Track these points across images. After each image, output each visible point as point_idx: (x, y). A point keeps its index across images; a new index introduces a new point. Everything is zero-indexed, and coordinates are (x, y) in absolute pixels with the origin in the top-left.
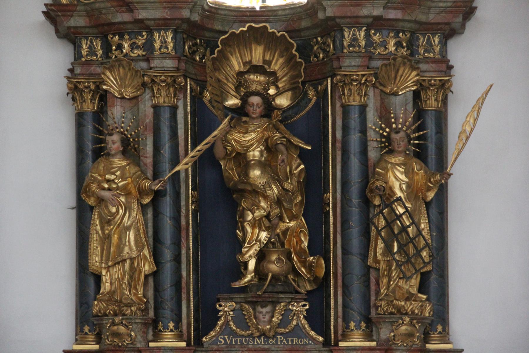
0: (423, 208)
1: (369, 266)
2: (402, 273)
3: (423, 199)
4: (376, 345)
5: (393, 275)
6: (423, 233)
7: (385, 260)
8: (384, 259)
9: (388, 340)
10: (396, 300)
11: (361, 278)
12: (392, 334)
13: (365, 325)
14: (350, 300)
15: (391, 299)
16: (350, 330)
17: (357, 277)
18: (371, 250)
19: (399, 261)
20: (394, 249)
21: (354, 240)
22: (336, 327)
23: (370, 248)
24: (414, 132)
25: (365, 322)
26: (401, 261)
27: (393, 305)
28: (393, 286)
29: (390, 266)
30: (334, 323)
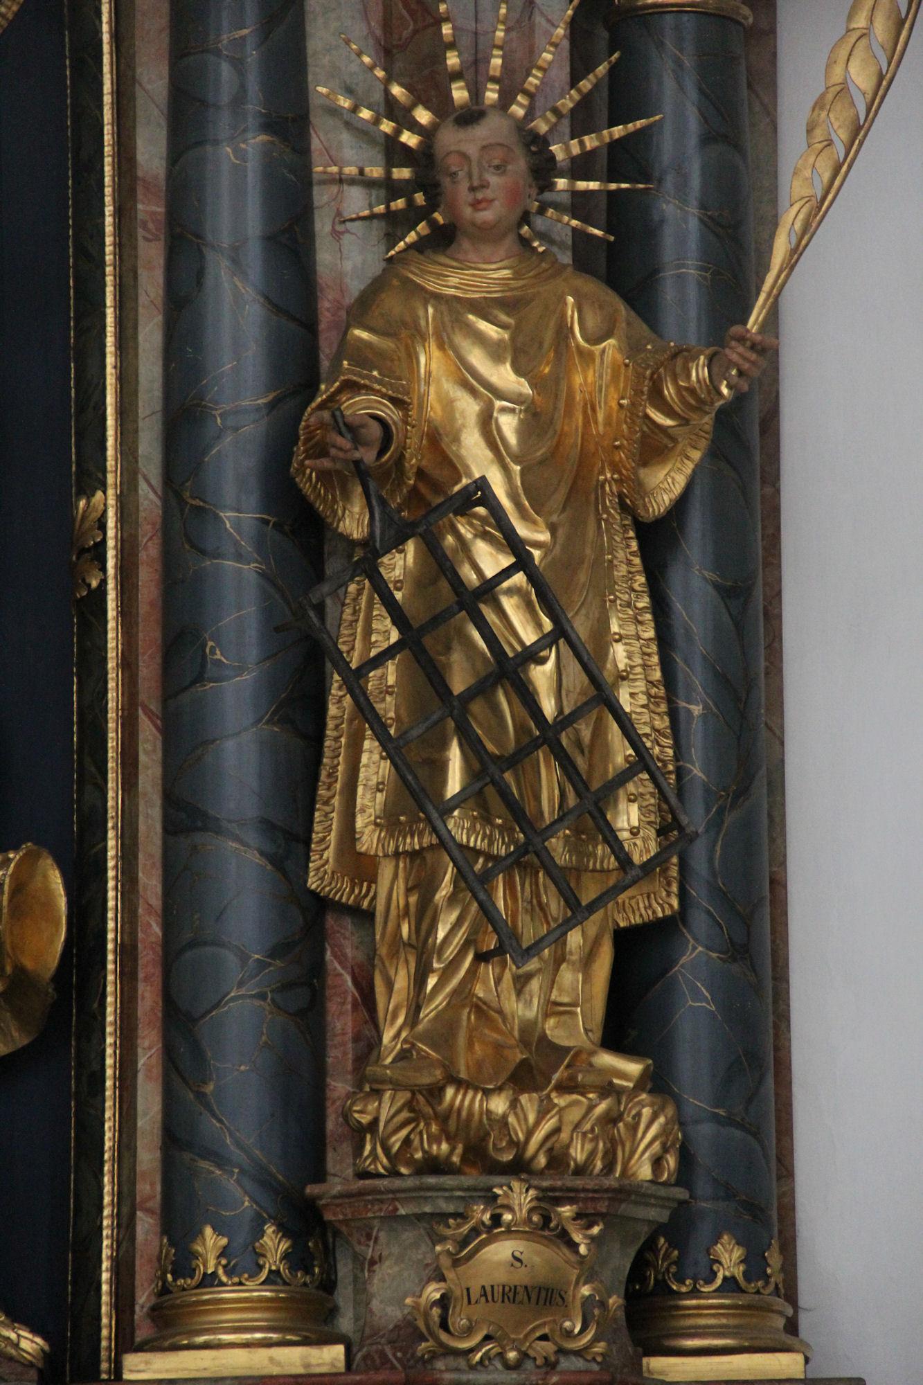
0: (621, 555)
1: (314, 894)
2: (495, 930)
3: (624, 508)
4: (341, 1366)
5: (441, 935)
6: (624, 698)
7: (397, 854)
8: (391, 849)
9: (409, 1332)
10: (460, 1084)
11: (262, 965)
12: (433, 1292)
13: (284, 1245)
14: (200, 1096)
15: (425, 1080)
16: (198, 1276)
17: (244, 958)
18: (327, 802)
19: (477, 853)
20: (444, 782)
21: (230, 745)
22: (124, 1269)
23: (322, 792)
24: (582, 120)
25: (284, 1230)
26: (489, 857)
27: (443, 1119)
28: (440, 1000)
29: (424, 886)
30: (118, 1243)
